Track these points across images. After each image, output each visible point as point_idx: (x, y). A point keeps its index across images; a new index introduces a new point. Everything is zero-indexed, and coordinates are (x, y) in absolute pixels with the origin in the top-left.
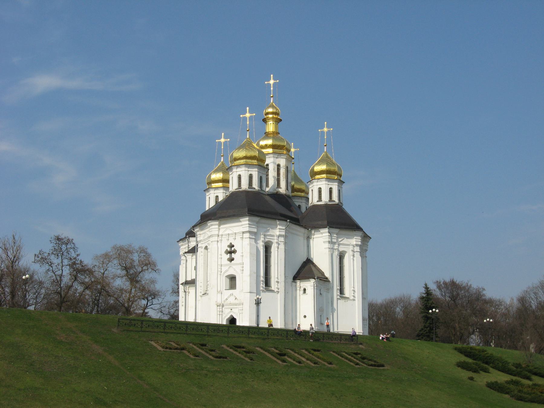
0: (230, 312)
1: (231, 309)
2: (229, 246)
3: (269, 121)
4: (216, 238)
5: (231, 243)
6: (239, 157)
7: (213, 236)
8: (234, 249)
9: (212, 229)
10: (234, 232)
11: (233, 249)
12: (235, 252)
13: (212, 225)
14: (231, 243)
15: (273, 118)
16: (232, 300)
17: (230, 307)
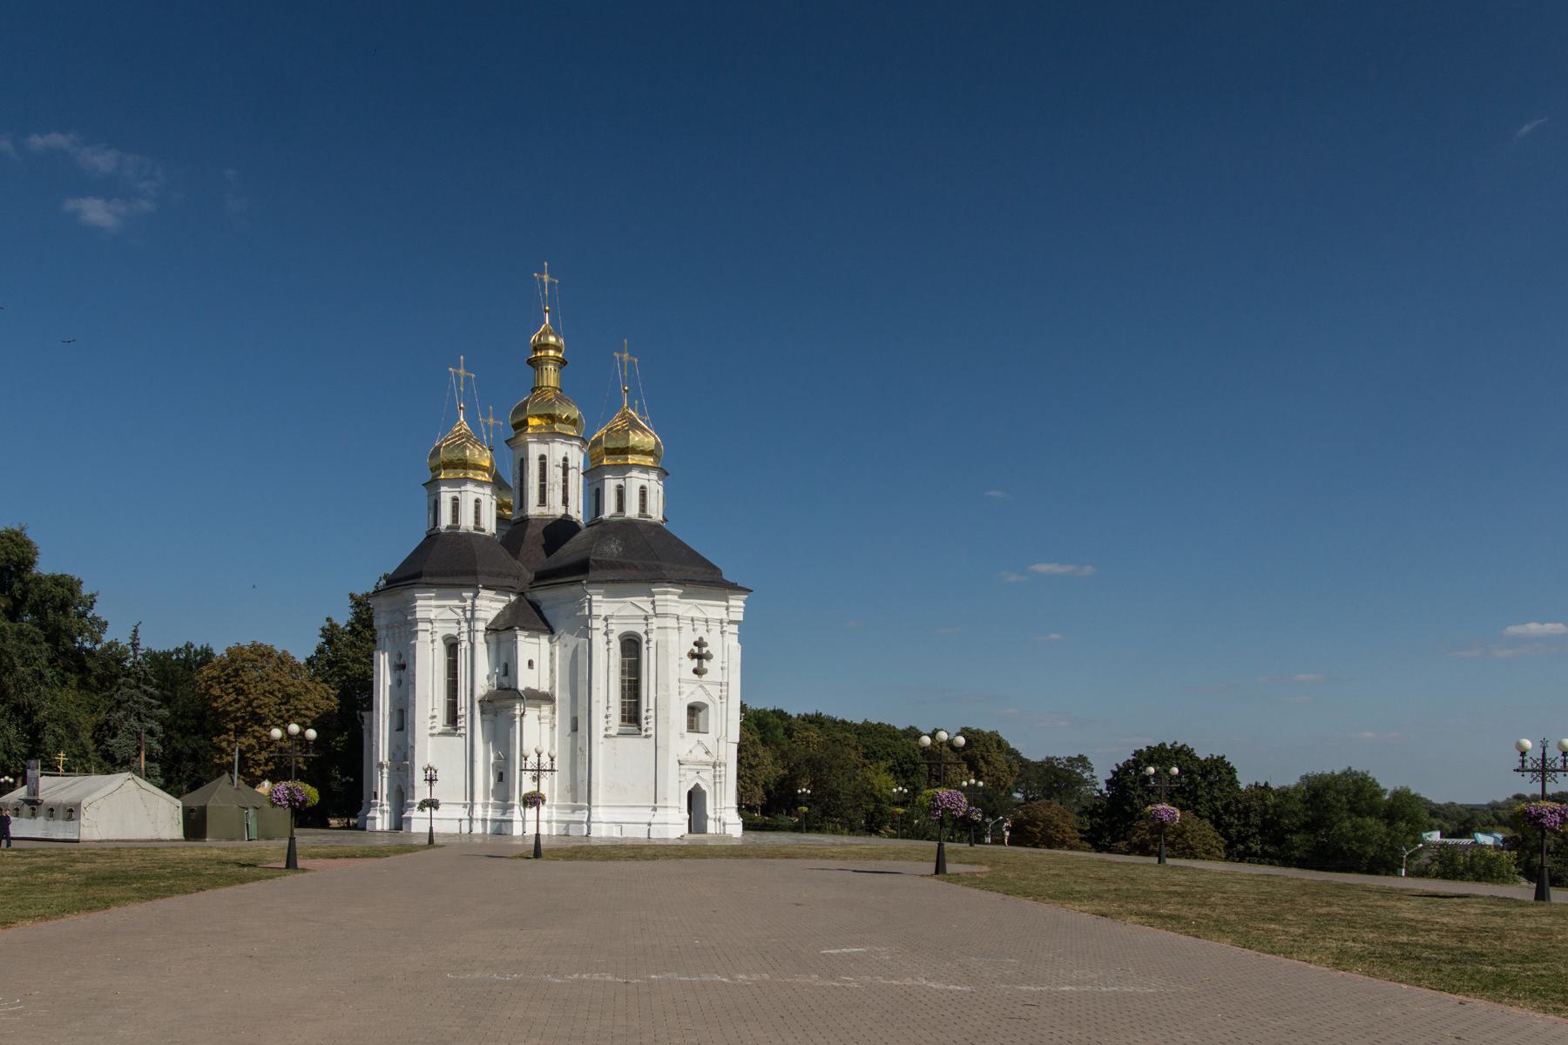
0: (696, 777)
1: (698, 773)
2: (695, 644)
3: (547, 364)
4: (672, 623)
5: (701, 639)
6: (642, 448)
7: (666, 617)
8: (708, 651)
9: (667, 600)
10: (709, 616)
11: (705, 650)
12: (708, 657)
13: (666, 593)
14: (701, 639)
15: (557, 359)
16: (700, 755)
17: (696, 767)
